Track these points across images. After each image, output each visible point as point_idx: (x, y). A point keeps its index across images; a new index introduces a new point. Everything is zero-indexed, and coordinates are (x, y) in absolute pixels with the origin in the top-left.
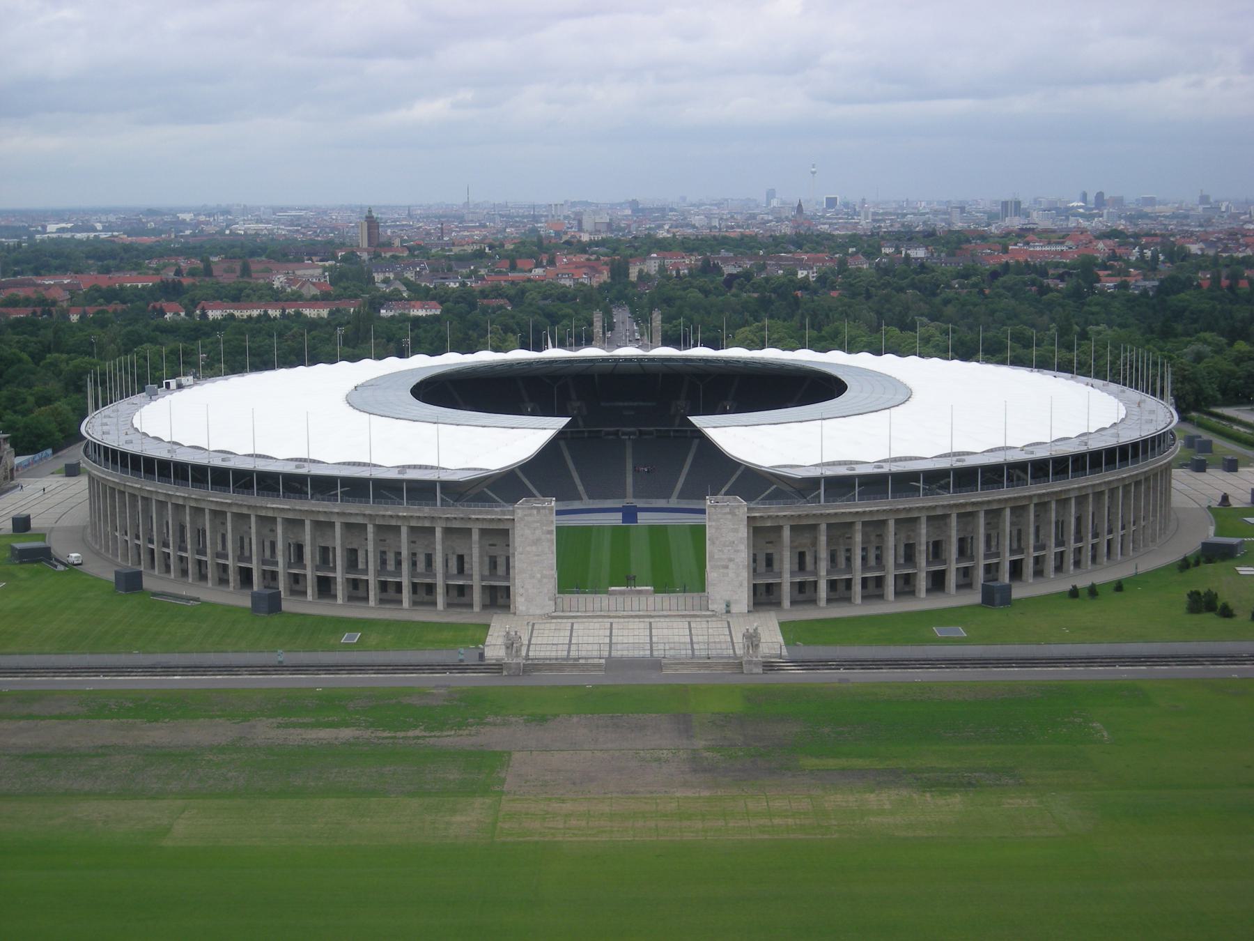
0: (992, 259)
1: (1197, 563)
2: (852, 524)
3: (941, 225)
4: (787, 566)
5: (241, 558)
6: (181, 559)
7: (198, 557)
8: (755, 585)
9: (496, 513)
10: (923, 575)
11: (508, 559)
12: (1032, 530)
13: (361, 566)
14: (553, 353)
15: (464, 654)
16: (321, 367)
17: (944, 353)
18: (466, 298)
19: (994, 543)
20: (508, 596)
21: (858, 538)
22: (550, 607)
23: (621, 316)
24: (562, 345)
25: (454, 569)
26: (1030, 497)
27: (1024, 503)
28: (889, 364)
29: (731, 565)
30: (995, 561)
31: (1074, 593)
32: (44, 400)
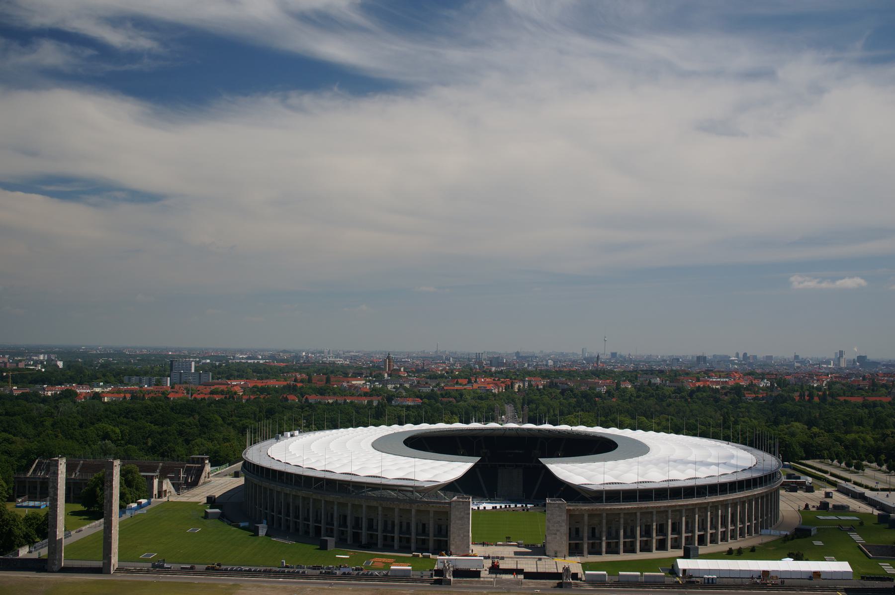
0: (689, 384)
1: (792, 539)
4: (586, 535)
10: (654, 541)
16: (360, 429)
17: (666, 430)
18: (431, 396)
23: (509, 408)
24: (479, 421)
32: (226, 440)
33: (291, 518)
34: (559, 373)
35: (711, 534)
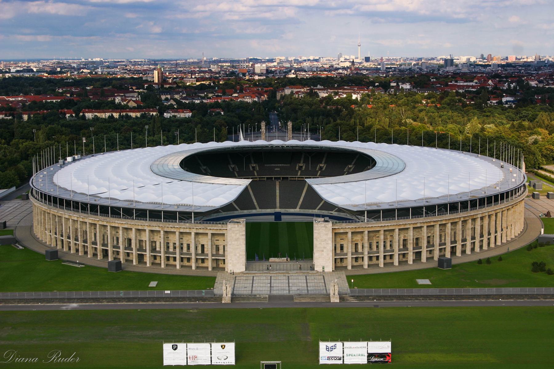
2: (378, 231)
5: (104, 245)
6: (76, 244)
7: (83, 244)
8: (335, 259)
9: (219, 227)
11: (224, 246)
12: (461, 232)
13: (158, 249)
15: (204, 293)
19: (443, 238)
20: (224, 263)
21: (382, 237)
22: (243, 269)
25: (200, 251)
26: (460, 218)
27: (457, 220)
29: (325, 250)
30: (444, 247)
31: (480, 262)
33: (80, 243)
35: (463, 245)
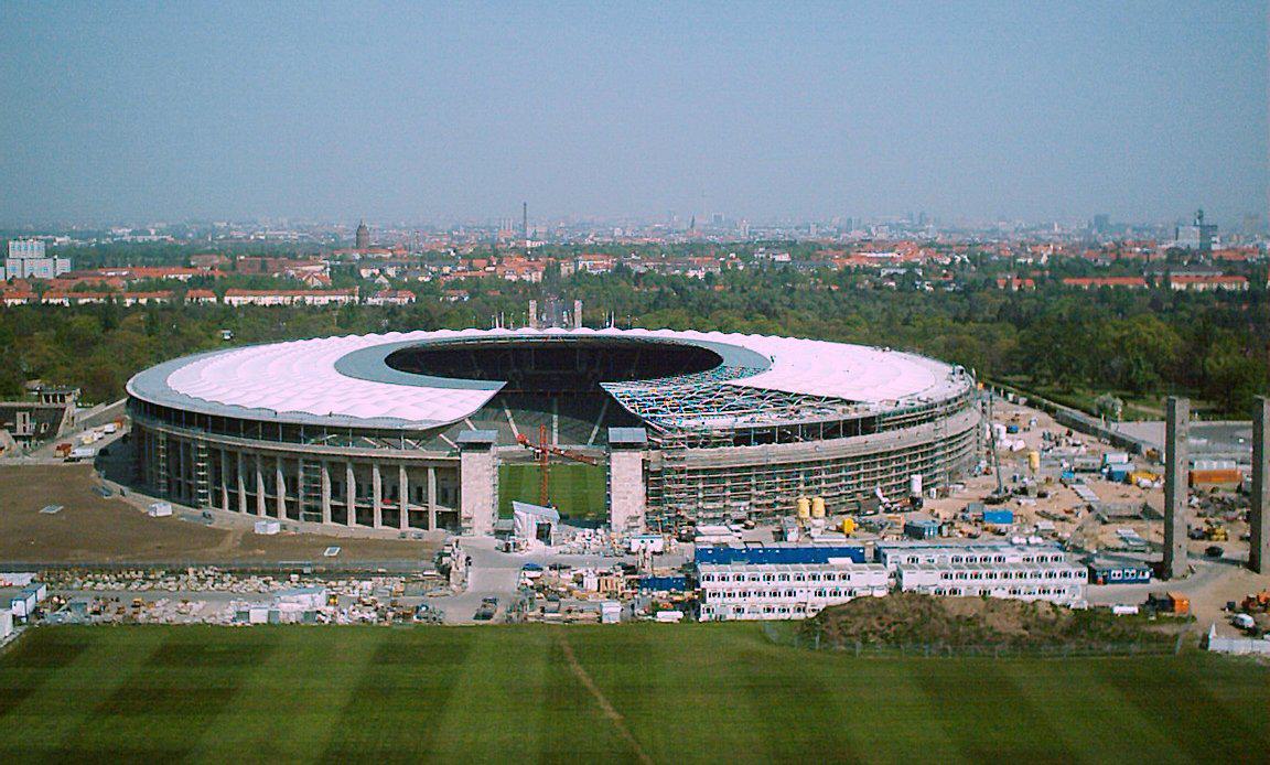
3: (800, 238)
14: (498, 332)
28: (755, 342)
29: (629, 497)
34: (633, 248)
